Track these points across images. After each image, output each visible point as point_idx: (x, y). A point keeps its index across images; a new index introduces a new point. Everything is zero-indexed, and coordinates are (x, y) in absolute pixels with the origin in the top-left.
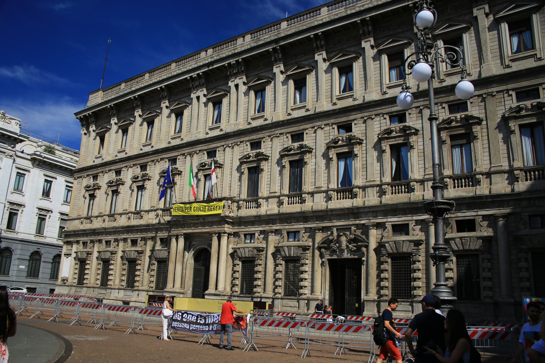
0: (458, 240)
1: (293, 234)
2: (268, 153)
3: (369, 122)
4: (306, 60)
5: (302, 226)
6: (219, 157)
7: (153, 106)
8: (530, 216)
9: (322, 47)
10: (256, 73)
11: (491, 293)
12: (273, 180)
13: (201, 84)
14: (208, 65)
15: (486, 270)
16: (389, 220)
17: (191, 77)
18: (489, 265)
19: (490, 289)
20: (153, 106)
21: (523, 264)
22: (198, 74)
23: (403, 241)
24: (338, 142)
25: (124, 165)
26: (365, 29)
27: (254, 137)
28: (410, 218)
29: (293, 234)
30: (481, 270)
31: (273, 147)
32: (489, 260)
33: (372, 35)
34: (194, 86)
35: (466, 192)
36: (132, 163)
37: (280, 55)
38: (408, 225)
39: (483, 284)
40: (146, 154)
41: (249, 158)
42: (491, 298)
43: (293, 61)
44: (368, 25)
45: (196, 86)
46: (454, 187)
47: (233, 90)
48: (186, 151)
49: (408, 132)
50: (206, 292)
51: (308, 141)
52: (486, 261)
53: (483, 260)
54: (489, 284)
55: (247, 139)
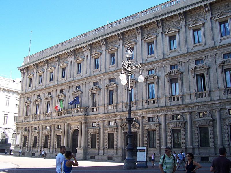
0: (172, 123)
5: (114, 119)
6: (81, 87)
16: (147, 115)
25: (41, 92)
28: (155, 114)
35: (176, 103)
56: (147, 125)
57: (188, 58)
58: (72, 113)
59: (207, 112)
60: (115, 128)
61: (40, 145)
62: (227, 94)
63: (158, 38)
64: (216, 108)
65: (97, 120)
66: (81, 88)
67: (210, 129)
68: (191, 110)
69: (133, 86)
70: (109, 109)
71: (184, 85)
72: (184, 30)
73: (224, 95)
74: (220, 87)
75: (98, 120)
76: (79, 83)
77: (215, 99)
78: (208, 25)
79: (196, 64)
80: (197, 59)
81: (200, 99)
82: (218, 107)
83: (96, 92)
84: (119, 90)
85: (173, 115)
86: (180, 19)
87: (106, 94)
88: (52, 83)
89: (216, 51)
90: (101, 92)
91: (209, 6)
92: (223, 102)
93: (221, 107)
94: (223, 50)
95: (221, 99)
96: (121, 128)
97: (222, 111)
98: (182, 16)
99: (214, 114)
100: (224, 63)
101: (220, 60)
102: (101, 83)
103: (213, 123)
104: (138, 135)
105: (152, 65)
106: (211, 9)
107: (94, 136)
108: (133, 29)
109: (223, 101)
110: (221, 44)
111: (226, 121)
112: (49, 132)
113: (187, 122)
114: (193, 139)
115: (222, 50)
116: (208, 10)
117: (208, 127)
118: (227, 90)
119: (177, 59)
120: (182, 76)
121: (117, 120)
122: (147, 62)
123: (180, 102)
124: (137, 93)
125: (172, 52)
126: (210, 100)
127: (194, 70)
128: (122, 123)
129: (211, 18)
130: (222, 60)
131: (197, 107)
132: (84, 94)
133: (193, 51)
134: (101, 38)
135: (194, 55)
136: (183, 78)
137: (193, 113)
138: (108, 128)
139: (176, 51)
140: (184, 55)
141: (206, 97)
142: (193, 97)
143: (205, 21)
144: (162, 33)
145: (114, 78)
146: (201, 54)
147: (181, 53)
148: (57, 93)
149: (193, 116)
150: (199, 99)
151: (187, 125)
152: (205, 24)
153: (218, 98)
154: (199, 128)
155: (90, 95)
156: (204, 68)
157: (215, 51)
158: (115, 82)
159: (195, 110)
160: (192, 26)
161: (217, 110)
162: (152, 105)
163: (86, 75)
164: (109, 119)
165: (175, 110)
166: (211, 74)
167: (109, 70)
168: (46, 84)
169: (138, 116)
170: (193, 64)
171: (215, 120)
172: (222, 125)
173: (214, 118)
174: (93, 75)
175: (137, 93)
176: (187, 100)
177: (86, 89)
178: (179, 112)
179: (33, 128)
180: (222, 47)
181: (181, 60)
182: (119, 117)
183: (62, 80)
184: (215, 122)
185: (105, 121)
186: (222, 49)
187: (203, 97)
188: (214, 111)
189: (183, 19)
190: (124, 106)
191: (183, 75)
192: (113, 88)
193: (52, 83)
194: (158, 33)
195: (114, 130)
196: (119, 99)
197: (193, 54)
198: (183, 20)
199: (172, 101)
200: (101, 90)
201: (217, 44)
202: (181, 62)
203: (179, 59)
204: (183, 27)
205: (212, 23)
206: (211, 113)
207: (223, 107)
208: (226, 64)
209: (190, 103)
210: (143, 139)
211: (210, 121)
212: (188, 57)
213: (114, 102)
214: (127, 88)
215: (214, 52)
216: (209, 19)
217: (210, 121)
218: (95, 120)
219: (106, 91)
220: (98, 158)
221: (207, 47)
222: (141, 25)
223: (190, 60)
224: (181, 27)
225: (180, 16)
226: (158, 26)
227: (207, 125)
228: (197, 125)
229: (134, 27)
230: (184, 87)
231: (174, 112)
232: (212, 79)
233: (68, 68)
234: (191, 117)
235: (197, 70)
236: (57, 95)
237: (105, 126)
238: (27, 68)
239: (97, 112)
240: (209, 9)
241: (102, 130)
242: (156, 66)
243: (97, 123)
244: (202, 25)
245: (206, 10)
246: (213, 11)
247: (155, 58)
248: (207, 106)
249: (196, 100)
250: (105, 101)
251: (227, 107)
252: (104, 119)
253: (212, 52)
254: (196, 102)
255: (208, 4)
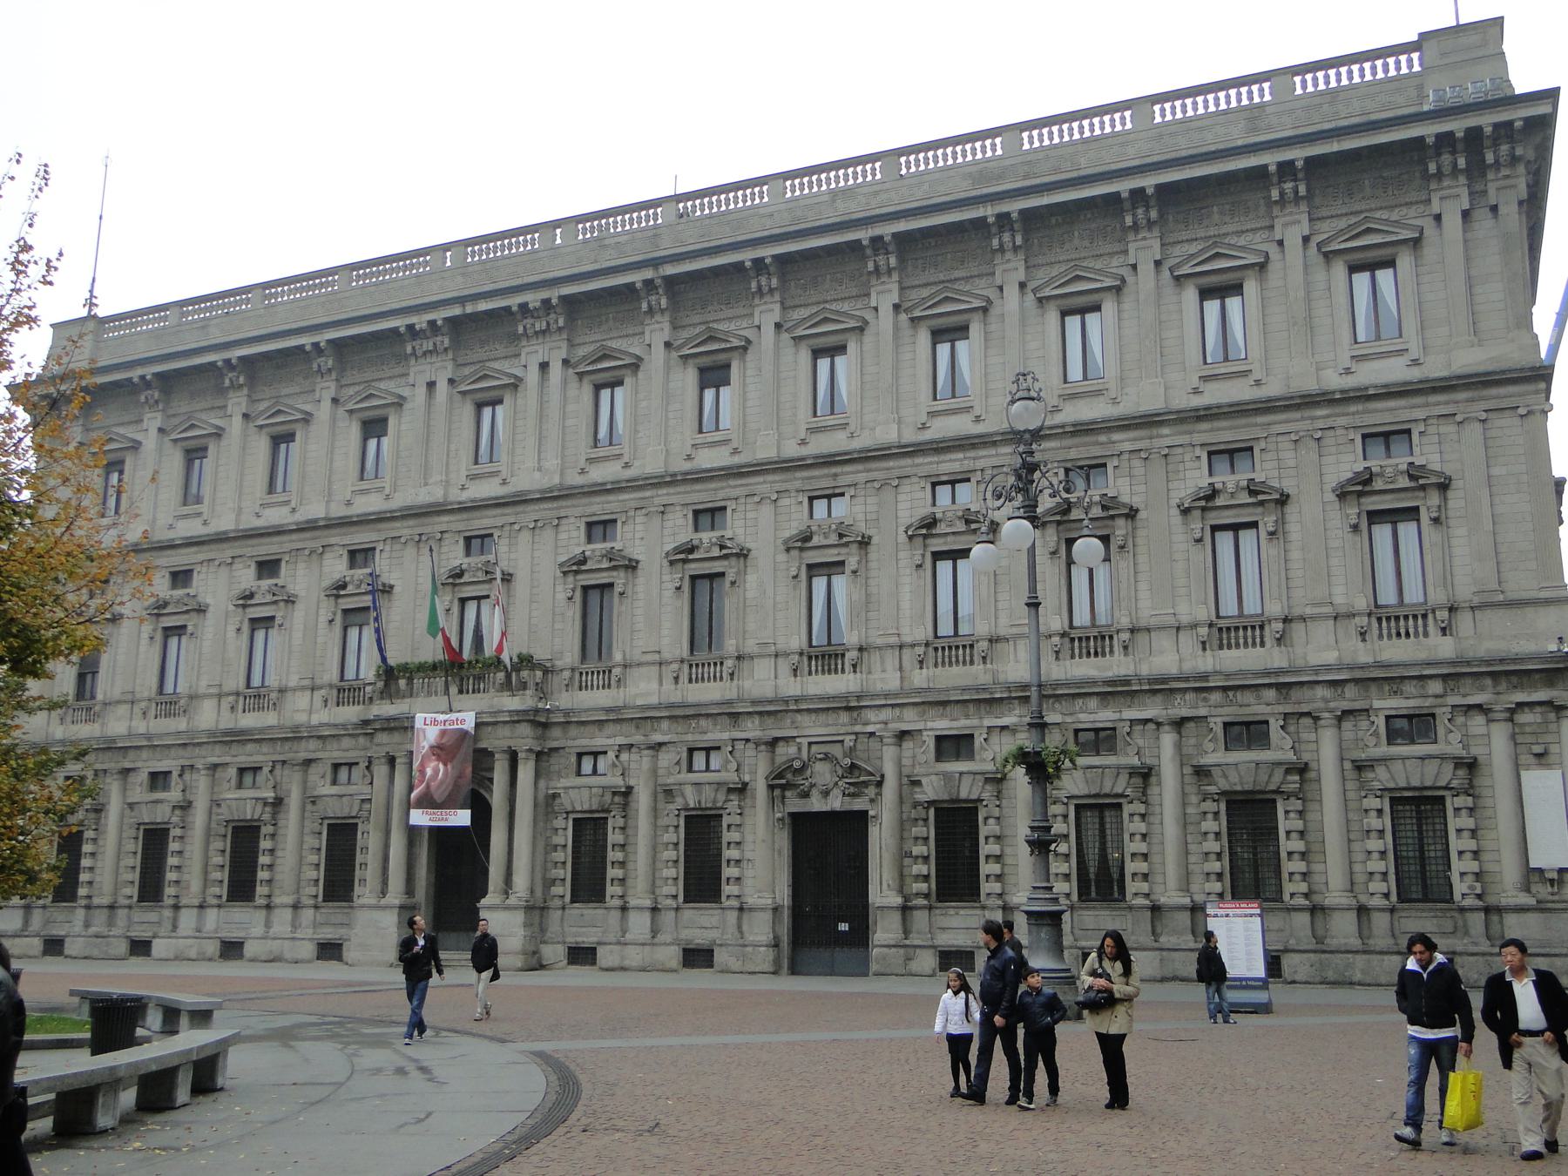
1: (703, 753)
2: (637, 552)
3: (888, 494)
4: (730, 319)
7: (285, 391)
8: (1226, 725)
9: (771, 291)
10: (597, 337)
11: (1145, 887)
12: (652, 617)
13: (440, 348)
14: (462, 300)
15: (1138, 837)
16: (930, 725)
17: (410, 327)
18: (1142, 827)
19: (1145, 877)
20: (285, 391)
21: (1209, 825)
22: (432, 323)
23: (961, 774)
24: (808, 539)
25: (201, 557)
26: (881, 260)
27: (599, 507)
28: (975, 722)
29: (703, 753)
30: (1126, 837)
31: (649, 538)
32: (1143, 816)
33: (895, 277)
34: (419, 352)
36: (230, 553)
37: (664, 302)
38: (972, 736)
39: (1131, 867)
40: (277, 532)
41: (584, 561)
42: (1147, 895)
43: (697, 319)
44: (887, 253)
45: (425, 354)
46: (1073, 657)
47: (533, 376)
48: (405, 529)
49: (973, 526)
50: (483, 901)
51: (736, 528)
52: (1136, 818)
53: (1131, 815)
54: (1143, 867)
55: (578, 511)
56: (934, 777)
57: (1167, 437)
58: (447, 692)
59: (1272, 721)
60: (730, 790)
61: (195, 885)
62: (1381, 636)
63: (994, 311)
64: (1321, 705)
65: (610, 741)
66: (505, 549)
67: (1287, 812)
68: (1185, 712)
69: (842, 563)
70: (690, 681)
71: (1141, 577)
72: (1152, 284)
73: (1364, 640)
74: (1339, 600)
75: (621, 740)
76: (486, 522)
77: (1315, 659)
78: (1291, 265)
79: (1211, 474)
80: (1222, 447)
81: (1234, 652)
82: (1332, 705)
83: (603, 578)
84: (752, 579)
85: (1077, 731)
86: (1135, 223)
87: (669, 593)
88: (287, 503)
89: (1328, 416)
90: (641, 580)
91: (1300, 175)
92: (1356, 681)
93: (1346, 705)
94: (1364, 412)
95: (1347, 660)
96: (771, 787)
97: (1347, 725)
98: (1147, 210)
99: (1304, 736)
100: (1368, 481)
101: (1346, 463)
102: (639, 527)
103: (1302, 781)
104: (874, 832)
105: (961, 455)
106: (1308, 190)
107: (589, 832)
108: (855, 246)
109: (1358, 674)
110: (1349, 382)
111: (1371, 775)
112: (265, 804)
113: (1159, 775)
114: (1192, 859)
115: (1358, 412)
116: (1296, 192)
117: (1274, 801)
118: (1379, 620)
119: (1103, 438)
120: (1134, 529)
121: (739, 746)
122: (927, 436)
123: (1116, 665)
124: (868, 602)
125: (1073, 396)
126: (1285, 664)
127: (1203, 503)
128: (773, 760)
129: (1306, 239)
130: (1359, 467)
131: (1216, 697)
132: (521, 586)
133: (1197, 402)
134: (648, 274)
135: (1205, 426)
136: (1139, 541)
137: (1192, 724)
138: (688, 790)
139: (1098, 393)
140: (1148, 422)
141: (1262, 644)
142: (1188, 641)
143: (1273, 250)
144: (1022, 285)
145: (724, 508)
146: (1243, 421)
147: (1127, 407)
148: (326, 570)
149: (1193, 741)
150: (1225, 653)
151: (1159, 784)
152: (1271, 267)
153: (1330, 657)
154: (1223, 806)
155: (561, 596)
156: (1261, 497)
157: (1320, 412)
158: (728, 534)
159: (1202, 712)
160: (1198, 269)
161: (1326, 715)
162: (955, 669)
163: (537, 475)
164: (690, 737)
165: (1093, 703)
166: (1294, 528)
167: (689, 458)
168: (240, 511)
169: (870, 729)
170: (1197, 473)
171: (1313, 765)
172: (1351, 795)
173: (1306, 757)
174: (579, 480)
175: (868, 602)
176: (1165, 658)
177: (536, 559)
178: (1117, 716)
179: (143, 776)
180: (1362, 396)
181: (1128, 446)
182: (752, 729)
183: (363, 492)
184: (1312, 775)
185: (660, 745)
186: (1360, 407)
187: (1246, 644)
188: (1307, 721)
189: (1150, 224)
190: (784, 666)
191: (1139, 524)
192: (717, 567)
193: (287, 503)
194: (1001, 288)
195: (721, 797)
196: (751, 626)
197: (1199, 419)
198: (1150, 229)
199: (1073, 657)
200: (639, 572)
201: (1334, 381)
202: (1126, 456)
203: (1116, 437)
204: (1146, 268)
205: (1306, 266)
206: (1292, 729)
207: (1357, 705)
208: (1378, 484)
209: (1174, 671)
210: (903, 855)
211: (1288, 771)
212: (1165, 431)
213: (730, 646)
214: (804, 568)
215: (1313, 418)
216: (1293, 237)
217: (1288, 771)
218: (599, 742)
219: (672, 578)
220: (623, 958)
221: (1273, 389)
222: (902, 226)
223: (1180, 450)
224: (1134, 267)
225: (1134, 208)
226: (1001, 245)
227: (1272, 787)
228: (1213, 789)
229: (863, 235)
230: (1143, 586)
231: (1082, 717)
232: (1295, 555)
233: (403, 427)
234: (1179, 746)
235: (1219, 502)
236: (327, 583)
237: (660, 772)
238: (54, 403)
239: (613, 692)
240: (1302, 190)
241: (643, 800)
242: (980, 464)
243: (611, 755)
244: (1250, 272)
245: (1282, 194)
246: (1317, 201)
247: (978, 419)
248: (1271, 694)
249: (1210, 661)
250: (665, 632)
251: (1377, 704)
252: (658, 737)
253: (1303, 419)
254: (1210, 668)
255: (1299, 164)
